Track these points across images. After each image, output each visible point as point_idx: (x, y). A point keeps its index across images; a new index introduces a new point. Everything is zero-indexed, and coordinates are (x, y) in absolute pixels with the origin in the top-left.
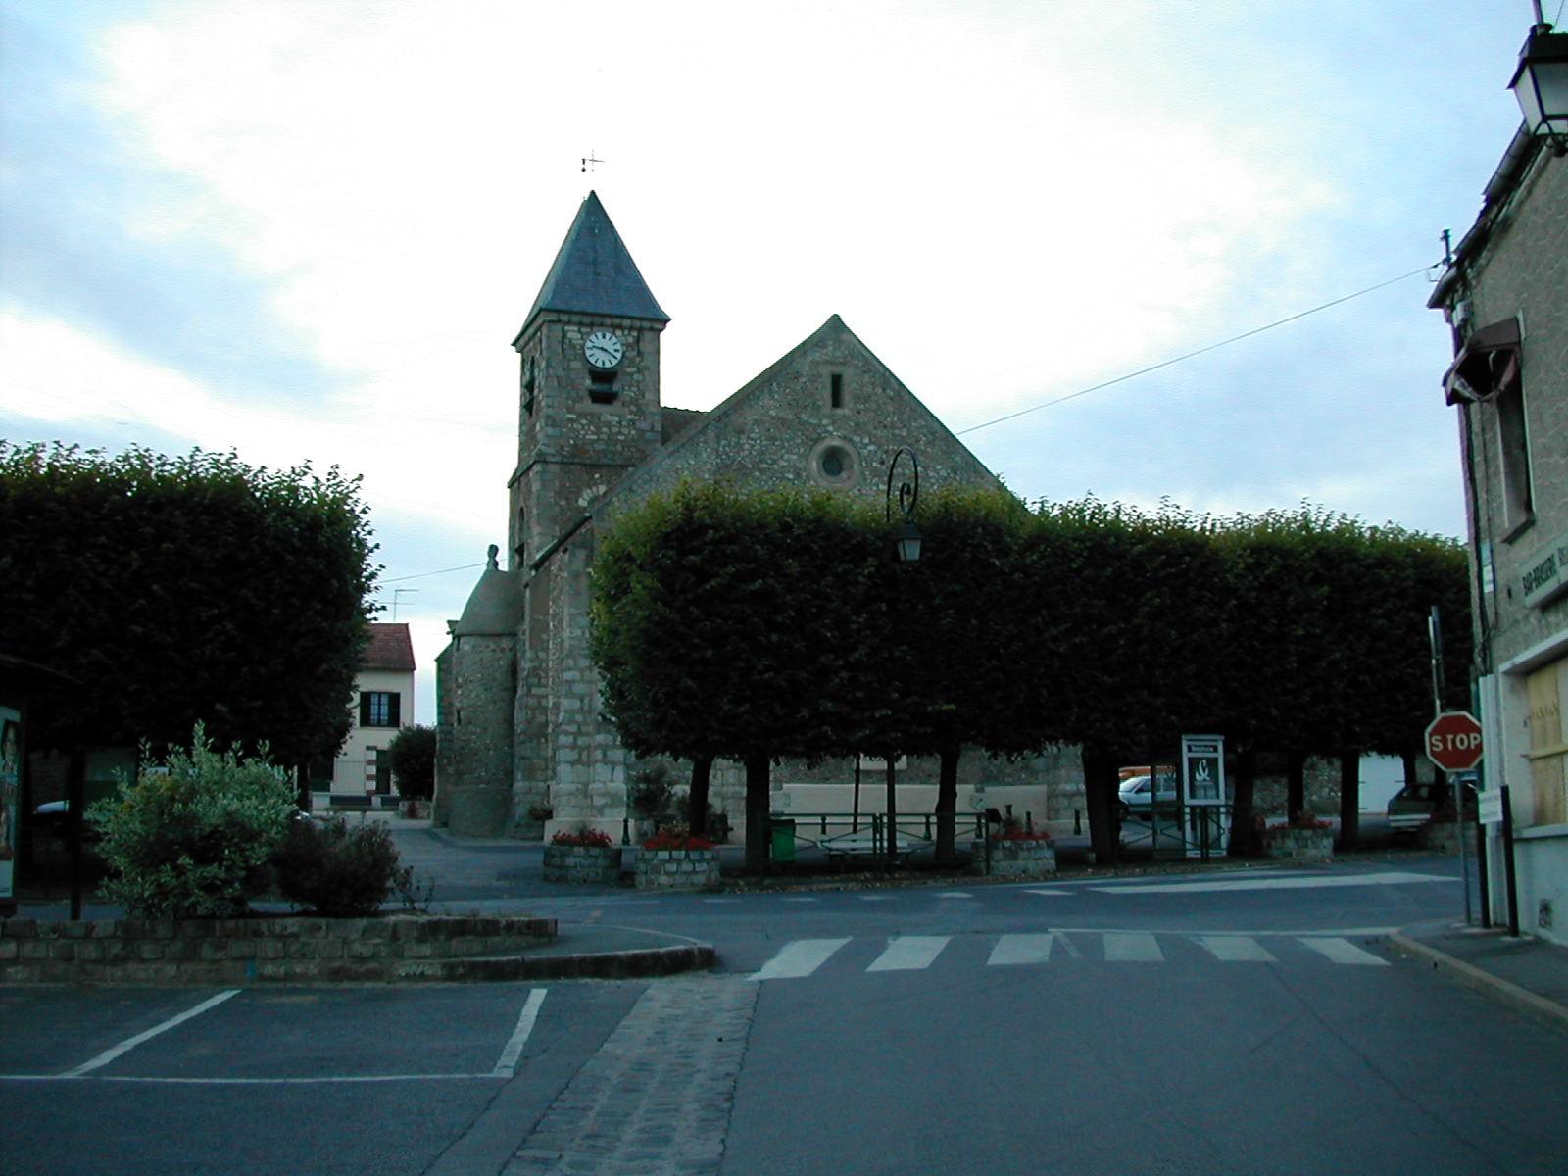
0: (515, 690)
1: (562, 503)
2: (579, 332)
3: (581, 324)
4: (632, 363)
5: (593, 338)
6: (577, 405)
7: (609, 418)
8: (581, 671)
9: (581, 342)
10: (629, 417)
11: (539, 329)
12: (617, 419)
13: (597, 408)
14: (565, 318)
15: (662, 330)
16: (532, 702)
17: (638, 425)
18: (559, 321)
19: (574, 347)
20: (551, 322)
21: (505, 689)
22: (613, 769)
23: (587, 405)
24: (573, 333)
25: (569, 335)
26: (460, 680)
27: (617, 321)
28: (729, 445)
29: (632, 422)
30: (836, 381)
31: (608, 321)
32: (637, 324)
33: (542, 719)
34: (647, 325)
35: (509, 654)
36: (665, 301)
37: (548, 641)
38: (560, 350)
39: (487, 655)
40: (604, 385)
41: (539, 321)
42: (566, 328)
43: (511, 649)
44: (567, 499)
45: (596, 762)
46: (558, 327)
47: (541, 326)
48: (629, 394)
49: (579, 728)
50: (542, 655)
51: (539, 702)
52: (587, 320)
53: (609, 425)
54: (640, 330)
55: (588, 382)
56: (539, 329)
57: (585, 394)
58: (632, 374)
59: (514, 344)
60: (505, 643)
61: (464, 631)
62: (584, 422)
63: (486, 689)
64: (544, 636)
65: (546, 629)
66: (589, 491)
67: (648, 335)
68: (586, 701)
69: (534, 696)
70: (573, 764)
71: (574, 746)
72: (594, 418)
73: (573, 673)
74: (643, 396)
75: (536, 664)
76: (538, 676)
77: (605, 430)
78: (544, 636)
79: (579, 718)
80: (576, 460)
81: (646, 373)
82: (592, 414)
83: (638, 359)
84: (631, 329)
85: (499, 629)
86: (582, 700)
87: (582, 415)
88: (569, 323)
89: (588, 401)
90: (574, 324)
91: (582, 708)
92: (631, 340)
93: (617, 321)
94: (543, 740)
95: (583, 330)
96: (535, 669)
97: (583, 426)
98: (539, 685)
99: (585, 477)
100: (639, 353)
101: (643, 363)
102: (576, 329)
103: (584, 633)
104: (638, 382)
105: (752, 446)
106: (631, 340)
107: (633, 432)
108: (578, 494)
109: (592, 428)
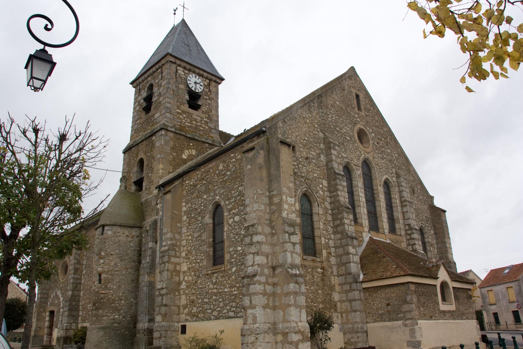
0: (140, 262)
1: (174, 154)
2: (184, 72)
3: (185, 68)
4: (206, 94)
5: (191, 76)
6: (182, 106)
7: (196, 117)
8: (266, 235)
9: (184, 77)
10: (205, 119)
11: (161, 67)
12: (200, 119)
13: (191, 111)
14: (178, 62)
15: (219, 84)
16: (171, 267)
17: (209, 124)
18: (175, 63)
19: (181, 78)
20: (171, 62)
21: (134, 261)
22: (300, 311)
23: (186, 107)
24: (181, 71)
25: (179, 71)
26: (103, 254)
27: (201, 72)
28: (323, 113)
29: (206, 123)
30: (357, 96)
31: (197, 70)
32: (210, 76)
33: (177, 279)
34: (214, 78)
35: (136, 239)
36: (221, 72)
37: (181, 228)
38: (175, 77)
39: (123, 238)
40: (194, 100)
41: (163, 62)
42: (178, 68)
43: (138, 237)
44: (177, 152)
45: (289, 306)
46: (174, 66)
47: (163, 65)
48: (204, 108)
49: (267, 279)
50: (177, 236)
51: (175, 267)
52: (188, 67)
53: (196, 120)
54: (211, 80)
55: (187, 97)
56: (161, 67)
57: (186, 102)
58: (207, 99)
59: (132, 83)
60: (135, 232)
61: (108, 223)
62: (185, 116)
63: (121, 260)
64: (179, 225)
65: (180, 221)
66: (187, 151)
67: (213, 84)
68: (270, 258)
69: (172, 263)
70: (265, 307)
71: (264, 294)
72: (190, 115)
73: (262, 236)
74: (211, 112)
75: (174, 242)
76: (175, 250)
77: (194, 122)
78: (179, 225)
79: (266, 271)
80: (183, 133)
81: (213, 101)
82: (189, 113)
83: (209, 93)
84: (207, 78)
85: (131, 222)
86: (267, 258)
87: (184, 112)
88: (179, 66)
89: (187, 106)
90: (182, 67)
91: (268, 263)
92: (206, 83)
93: (201, 72)
94: (177, 294)
95: (186, 71)
96: (173, 245)
97: (184, 117)
98: (176, 256)
99: (186, 143)
100: (210, 91)
101: (211, 96)
102: (182, 70)
103: (266, 208)
104: (209, 104)
105: (332, 117)
106: (206, 83)
107: (207, 127)
108: (182, 152)
109: (188, 120)
